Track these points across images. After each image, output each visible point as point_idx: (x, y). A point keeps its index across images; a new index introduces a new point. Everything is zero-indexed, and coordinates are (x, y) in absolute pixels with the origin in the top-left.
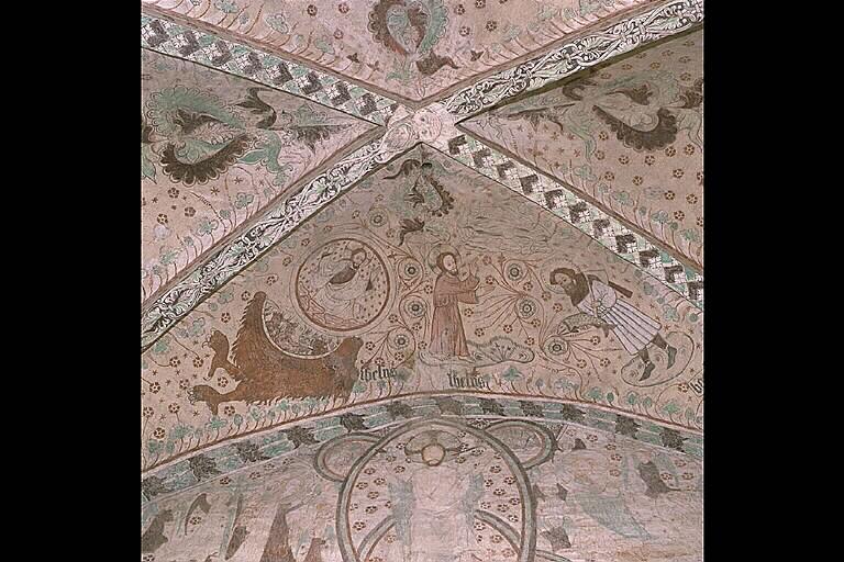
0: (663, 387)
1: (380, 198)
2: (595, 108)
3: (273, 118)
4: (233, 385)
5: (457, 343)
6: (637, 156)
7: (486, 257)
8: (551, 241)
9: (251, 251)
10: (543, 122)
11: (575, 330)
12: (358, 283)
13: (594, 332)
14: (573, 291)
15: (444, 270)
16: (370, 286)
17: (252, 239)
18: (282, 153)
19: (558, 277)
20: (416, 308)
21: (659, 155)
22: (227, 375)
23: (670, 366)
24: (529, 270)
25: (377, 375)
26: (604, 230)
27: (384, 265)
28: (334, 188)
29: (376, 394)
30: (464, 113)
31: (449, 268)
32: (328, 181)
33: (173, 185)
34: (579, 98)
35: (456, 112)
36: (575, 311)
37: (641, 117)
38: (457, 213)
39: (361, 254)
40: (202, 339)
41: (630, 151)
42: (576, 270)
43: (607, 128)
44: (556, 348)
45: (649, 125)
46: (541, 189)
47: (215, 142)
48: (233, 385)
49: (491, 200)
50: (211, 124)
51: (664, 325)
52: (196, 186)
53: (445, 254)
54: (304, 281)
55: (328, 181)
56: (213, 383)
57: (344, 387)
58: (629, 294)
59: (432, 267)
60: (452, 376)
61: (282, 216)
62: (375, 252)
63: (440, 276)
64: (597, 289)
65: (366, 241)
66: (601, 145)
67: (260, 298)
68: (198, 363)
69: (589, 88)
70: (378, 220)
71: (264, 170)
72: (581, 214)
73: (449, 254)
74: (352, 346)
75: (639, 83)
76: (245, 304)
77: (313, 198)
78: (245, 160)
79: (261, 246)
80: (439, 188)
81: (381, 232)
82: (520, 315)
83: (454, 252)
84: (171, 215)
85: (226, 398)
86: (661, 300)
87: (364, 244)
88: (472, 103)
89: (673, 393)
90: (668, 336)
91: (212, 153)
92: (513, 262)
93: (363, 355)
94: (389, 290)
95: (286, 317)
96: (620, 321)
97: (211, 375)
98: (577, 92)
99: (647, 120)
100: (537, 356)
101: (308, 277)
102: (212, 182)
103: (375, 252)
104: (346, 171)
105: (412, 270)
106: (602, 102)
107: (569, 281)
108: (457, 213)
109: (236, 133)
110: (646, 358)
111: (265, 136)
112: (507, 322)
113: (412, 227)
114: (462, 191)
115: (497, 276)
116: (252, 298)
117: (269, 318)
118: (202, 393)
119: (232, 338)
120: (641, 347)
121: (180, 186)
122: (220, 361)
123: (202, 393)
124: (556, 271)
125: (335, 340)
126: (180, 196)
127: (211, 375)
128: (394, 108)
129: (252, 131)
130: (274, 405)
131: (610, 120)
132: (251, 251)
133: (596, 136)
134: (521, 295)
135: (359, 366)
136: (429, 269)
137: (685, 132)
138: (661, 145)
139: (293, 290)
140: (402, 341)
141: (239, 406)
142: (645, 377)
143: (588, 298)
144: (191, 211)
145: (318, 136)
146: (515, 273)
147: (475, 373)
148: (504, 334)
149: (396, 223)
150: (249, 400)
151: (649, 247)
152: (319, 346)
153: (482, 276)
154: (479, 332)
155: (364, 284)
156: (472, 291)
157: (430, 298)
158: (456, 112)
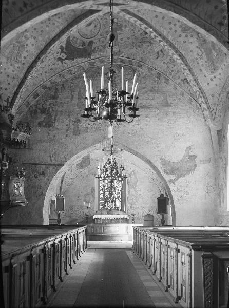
12: (93, 26)
13: (148, 44)
16: (95, 26)
44: (139, 46)
48: (65, 56)
56: (61, 57)
57: (89, 55)
68: (58, 53)
74: (91, 42)
84: (49, 25)
89: (162, 64)
93: (94, 46)
110: (158, 54)
118: (60, 59)
122: (62, 52)
123: (60, 59)
130: (74, 61)
134: (133, 30)
135: (93, 49)
140: (103, 42)
141: (67, 61)
142: (157, 58)
144: (54, 24)
147: (120, 51)
148: (127, 40)
150: (69, 60)
152: (84, 44)
153: (124, 24)
154: (122, 39)
155: (94, 26)
156: (121, 28)
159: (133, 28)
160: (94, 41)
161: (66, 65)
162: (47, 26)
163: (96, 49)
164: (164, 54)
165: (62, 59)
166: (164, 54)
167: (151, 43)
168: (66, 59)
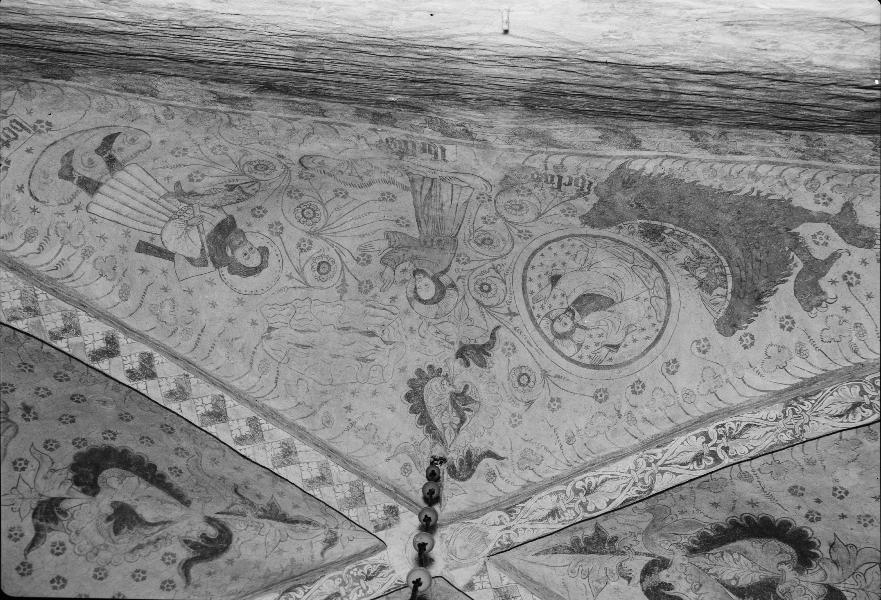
0: (80, 127)
1: (515, 420)
2: (187, 503)
3: (647, 571)
4: (805, 230)
5: (425, 188)
6: (126, 440)
7: (366, 292)
8: (261, 329)
9: (720, 437)
10: (262, 503)
11: (231, 188)
13: (200, 187)
14: (232, 236)
15: (436, 279)
16: (555, 280)
17: (713, 454)
18: (644, 526)
19: (254, 260)
20: (486, 242)
21: (96, 439)
22: (810, 242)
23: (70, 154)
24: (300, 271)
25: (565, 180)
26: (173, 387)
27: (527, 305)
28: (577, 492)
29: (571, 162)
30: (370, 563)
31: (427, 280)
32: (584, 506)
33: (811, 525)
34: (210, 521)
35: (383, 567)
36: (230, 210)
37: (119, 487)
38: (403, 370)
39: (559, 328)
40: (834, 310)
41: (136, 448)
42: (228, 276)
43: (171, 479)
45: (111, 476)
46: (268, 447)
47: (736, 556)
48: (805, 230)
49: (347, 399)
50: (733, 583)
51: (83, 212)
52: (778, 515)
53: (434, 301)
54: (653, 320)
55: (584, 506)
56: (837, 243)
58: (145, 248)
59: (453, 286)
60: (438, 154)
61: (662, 472)
62: (537, 326)
63: (444, 272)
64: (191, 244)
65: (546, 348)
66: (181, 463)
67: (730, 324)
69: (194, 536)
70: (523, 378)
71: (675, 510)
72: (209, 408)
73: (425, 302)
75: (126, 541)
76: (752, 328)
77: (609, 486)
78: (699, 525)
79: (702, 439)
80: (425, 420)
81: (523, 357)
82: (320, 206)
83: (417, 304)
84: (826, 495)
85: (824, 218)
86: (86, 254)
87: (551, 344)
88: (357, 579)
90: (74, 196)
91: (744, 544)
92: (325, 285)
93: (585, 205)
94: (526, 269)
95: (694, 281)
96: (154, 205)
97: (835, 256)
98: (212, 532)
99: (114, 482)
100: (296, 159)
101: (646, 323)
102: (756, 513)
103: (537, 326)
104: (554, 513)
105: (485, 288)
106: (175, 511)
107: (239, 253)
108: (403, 370)
109: (701, 560)
110: (111, 161)
111: (663, 549)
112: (343, 202)
113: (474, 353)
114: (389, 415)
115: (352, 265)
116: (739, 333)
117: (720, 291)
119: (786, 289)
120: (120, 174)
121: (800, 522)
122: (816, 269)
124: (257, 270)
125: (625, 231)
126: (804, 512)
127: (835, 256)
128: (470, 586)
129: (678, 558)
130: (746, 186)
131: (168, 488)
132: (720, 437)
133: (186, 474)
134: (315, 234)
135: (593, 198)
136: (459, 284)
137: (59, 466)
138: (93, 451)
139: (673, 318)
143: (208, 228)
145: (588, 541)
146: (323, 267)
149: (498, 360)
151: (103, 365)
153: (376, 265)
155: (562, 284)
156: (394, 248)
157: (462, 248)
158: (383, 567)
159: (318, 243)
160: (576, 222)
161: (826, 189)
162: (841, 494)
163: (572, 190)
164: (67, 173)
165: (836, 227)
166: (67, 173)
167: (180, 194)
168: (810, 218)
